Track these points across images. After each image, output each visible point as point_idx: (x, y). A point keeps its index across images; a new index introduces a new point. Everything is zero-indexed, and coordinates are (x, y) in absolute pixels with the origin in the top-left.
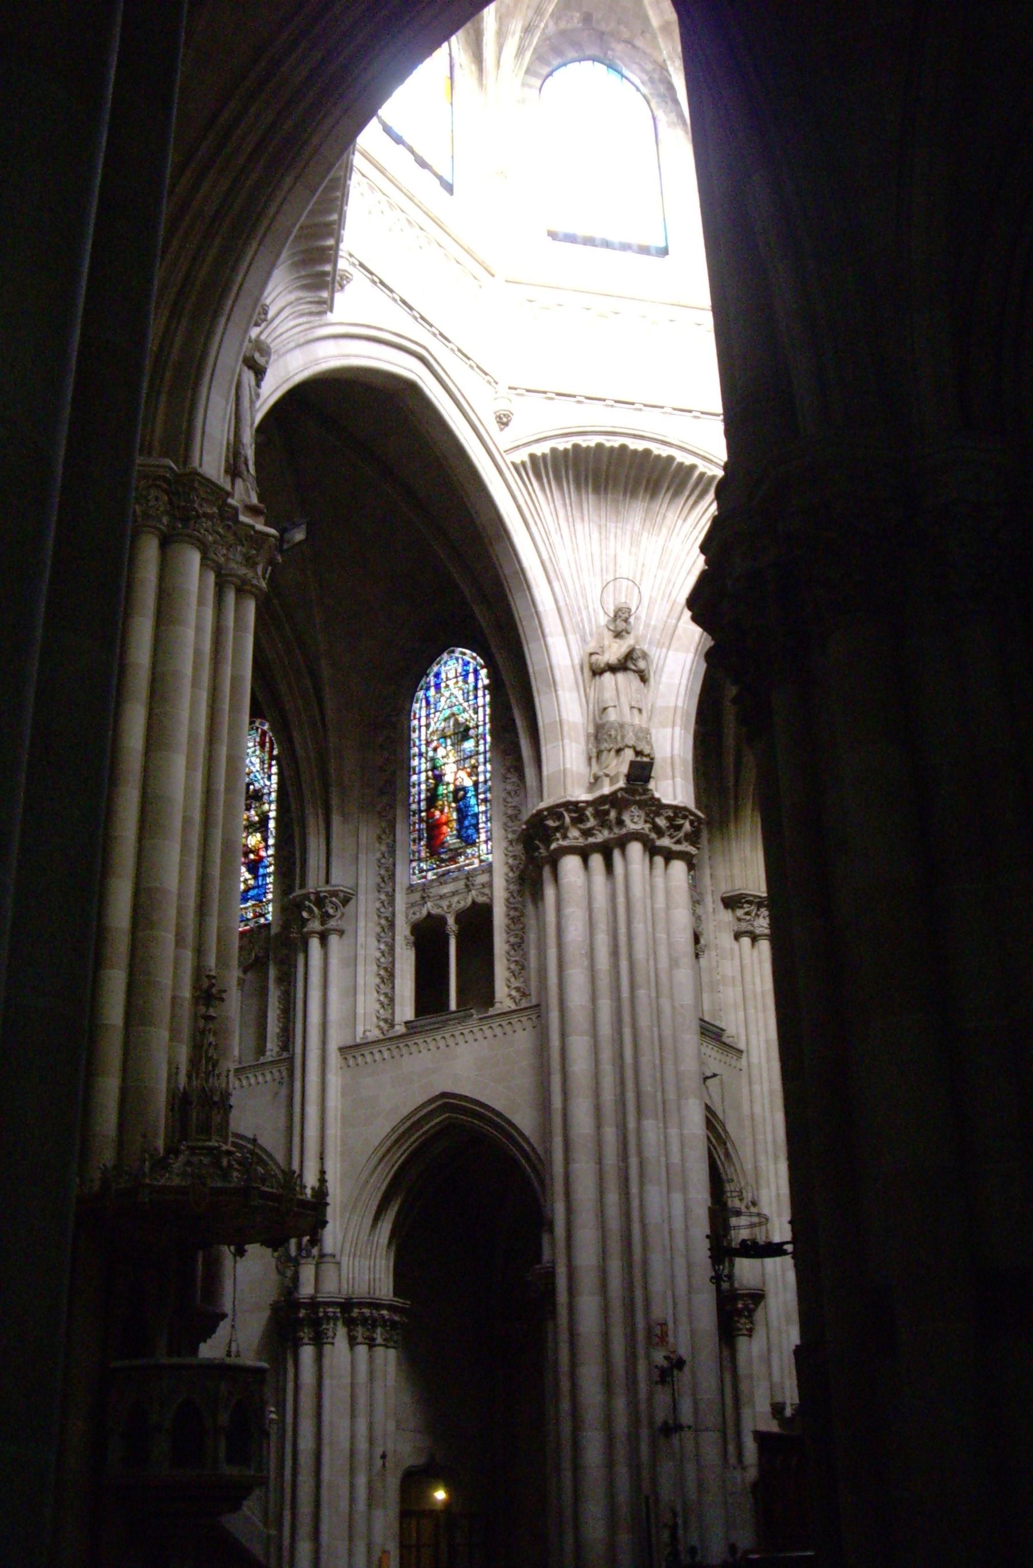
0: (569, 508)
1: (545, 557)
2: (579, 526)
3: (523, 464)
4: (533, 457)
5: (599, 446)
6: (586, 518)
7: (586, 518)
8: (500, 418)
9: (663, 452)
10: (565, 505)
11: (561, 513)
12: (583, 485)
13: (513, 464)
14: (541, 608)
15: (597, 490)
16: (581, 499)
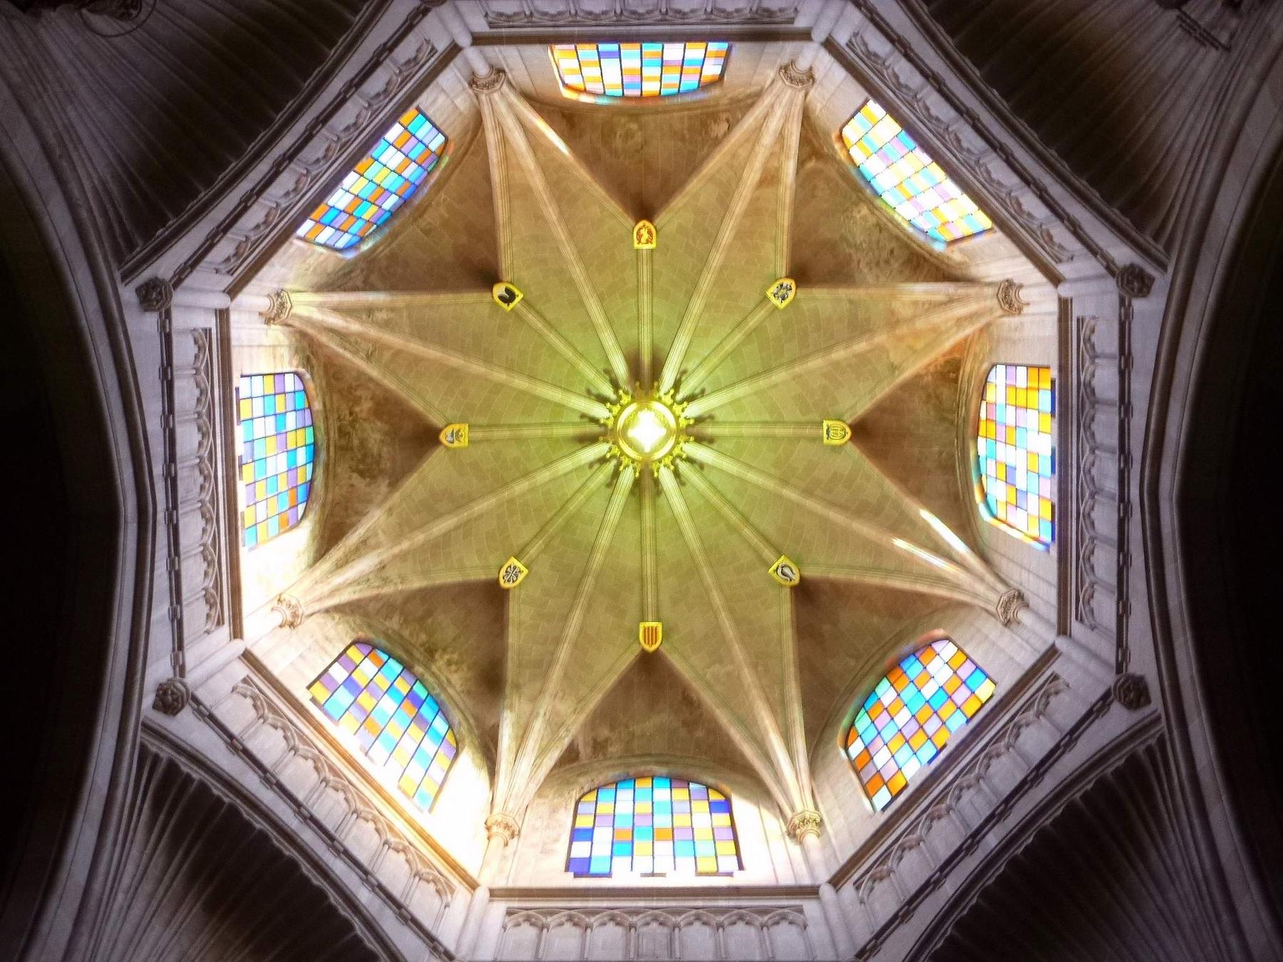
0: (161, 890)
1: (97, 886)
2: (157, 926)
3: (156, 758)
4: (172, 765)
5: (263, 836)
6: (174, 926)
7: (174, 926)
8: (165, 693)
9: (344, 911)
10: (160, 881)
11: (147, 887)
12: (196, 887)
13: (143, 747)
14: (44, 928)
15: (211, 907)
16: (184, 898)
